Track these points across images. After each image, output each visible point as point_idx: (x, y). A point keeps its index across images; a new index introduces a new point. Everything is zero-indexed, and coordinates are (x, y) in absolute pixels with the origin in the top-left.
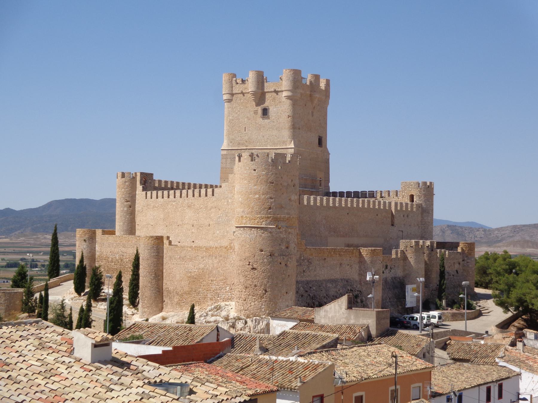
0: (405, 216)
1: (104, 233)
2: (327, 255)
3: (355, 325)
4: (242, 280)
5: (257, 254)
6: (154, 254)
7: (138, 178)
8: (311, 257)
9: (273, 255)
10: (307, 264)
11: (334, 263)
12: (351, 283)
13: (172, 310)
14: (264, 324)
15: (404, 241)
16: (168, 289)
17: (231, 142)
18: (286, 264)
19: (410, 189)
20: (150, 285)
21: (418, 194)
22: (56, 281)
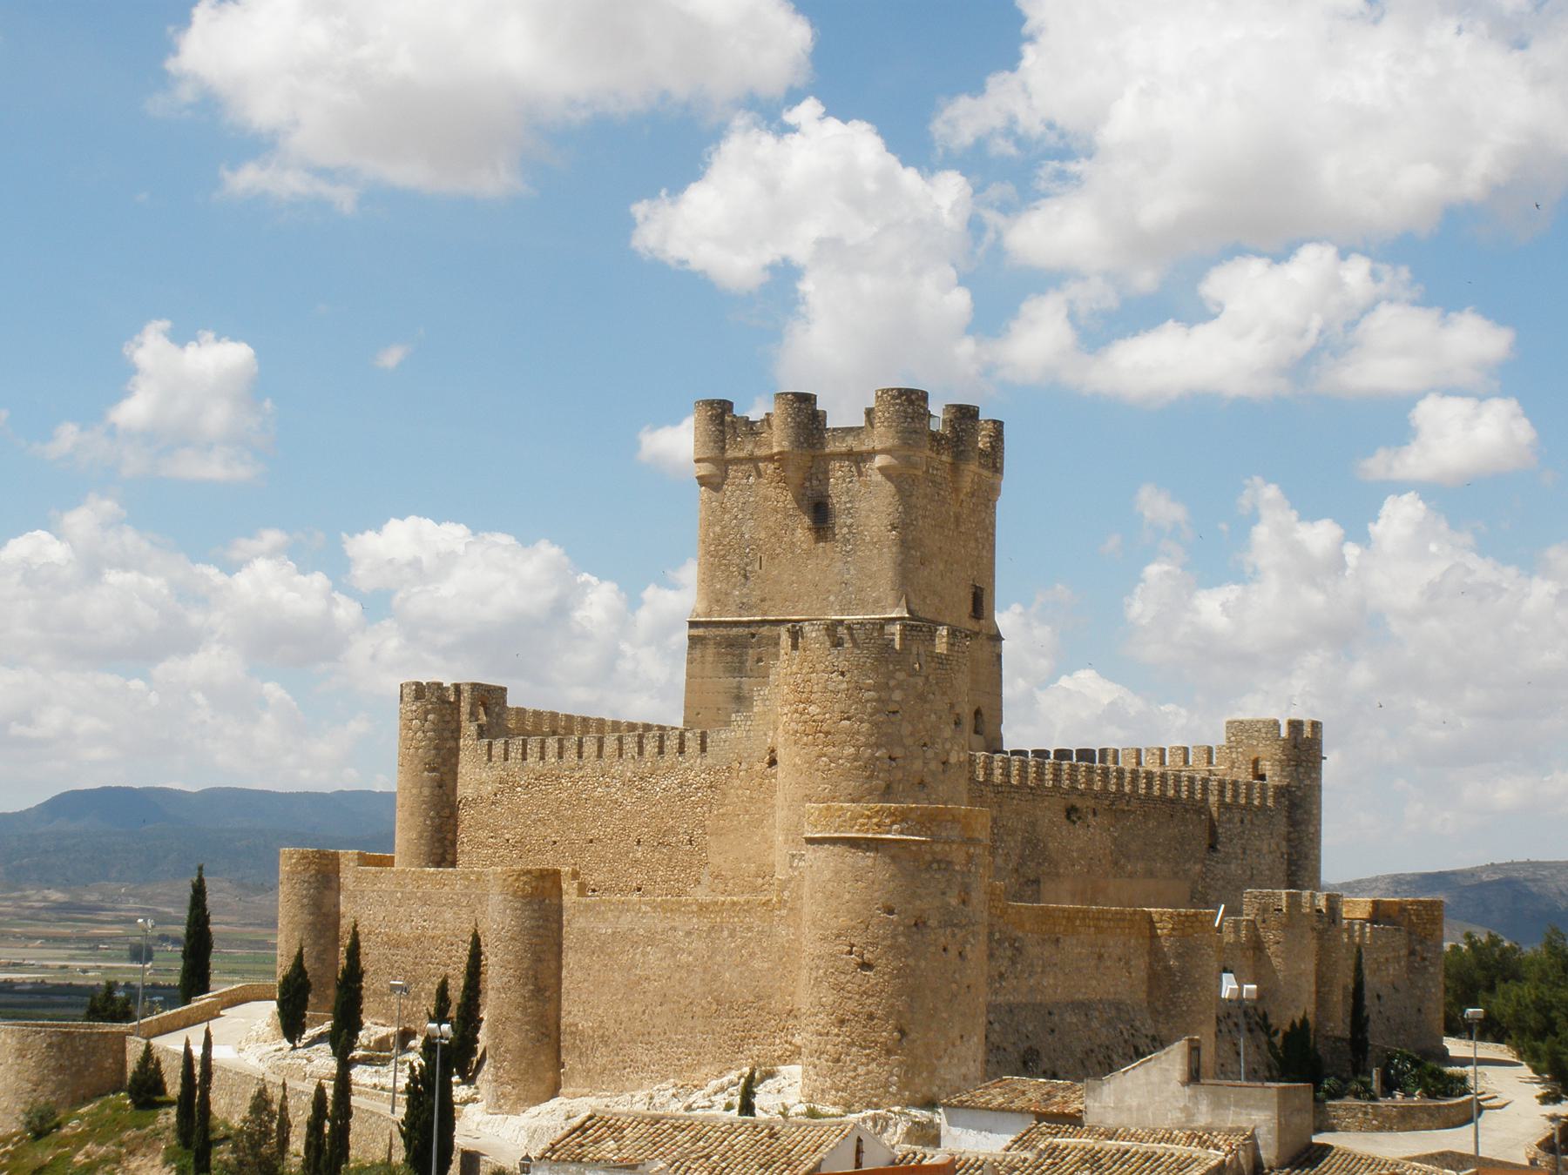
0: (1246, 821)
1: (364, 860)
2: (1062, 929)
3: (1214, 1129)
4: (828, 1000)
5: (875, 921)
6: (533, 923)
7: (466, 695)
8: (1020, 935)
9: (924, 923)
10: (1009, 953)
11: (1080, 953)
12: (1128, 1012)
13: (587, 1090)
14: (899, 1131)
15: (1256, 892)
16: (574, 1029)
17: (718, 601)
18: (960, 953)
19: (1255, 743)
20: (519, 1015)
21: (1280, 756)
22: (207, 1004)
